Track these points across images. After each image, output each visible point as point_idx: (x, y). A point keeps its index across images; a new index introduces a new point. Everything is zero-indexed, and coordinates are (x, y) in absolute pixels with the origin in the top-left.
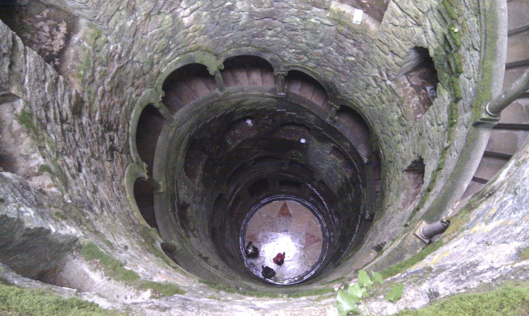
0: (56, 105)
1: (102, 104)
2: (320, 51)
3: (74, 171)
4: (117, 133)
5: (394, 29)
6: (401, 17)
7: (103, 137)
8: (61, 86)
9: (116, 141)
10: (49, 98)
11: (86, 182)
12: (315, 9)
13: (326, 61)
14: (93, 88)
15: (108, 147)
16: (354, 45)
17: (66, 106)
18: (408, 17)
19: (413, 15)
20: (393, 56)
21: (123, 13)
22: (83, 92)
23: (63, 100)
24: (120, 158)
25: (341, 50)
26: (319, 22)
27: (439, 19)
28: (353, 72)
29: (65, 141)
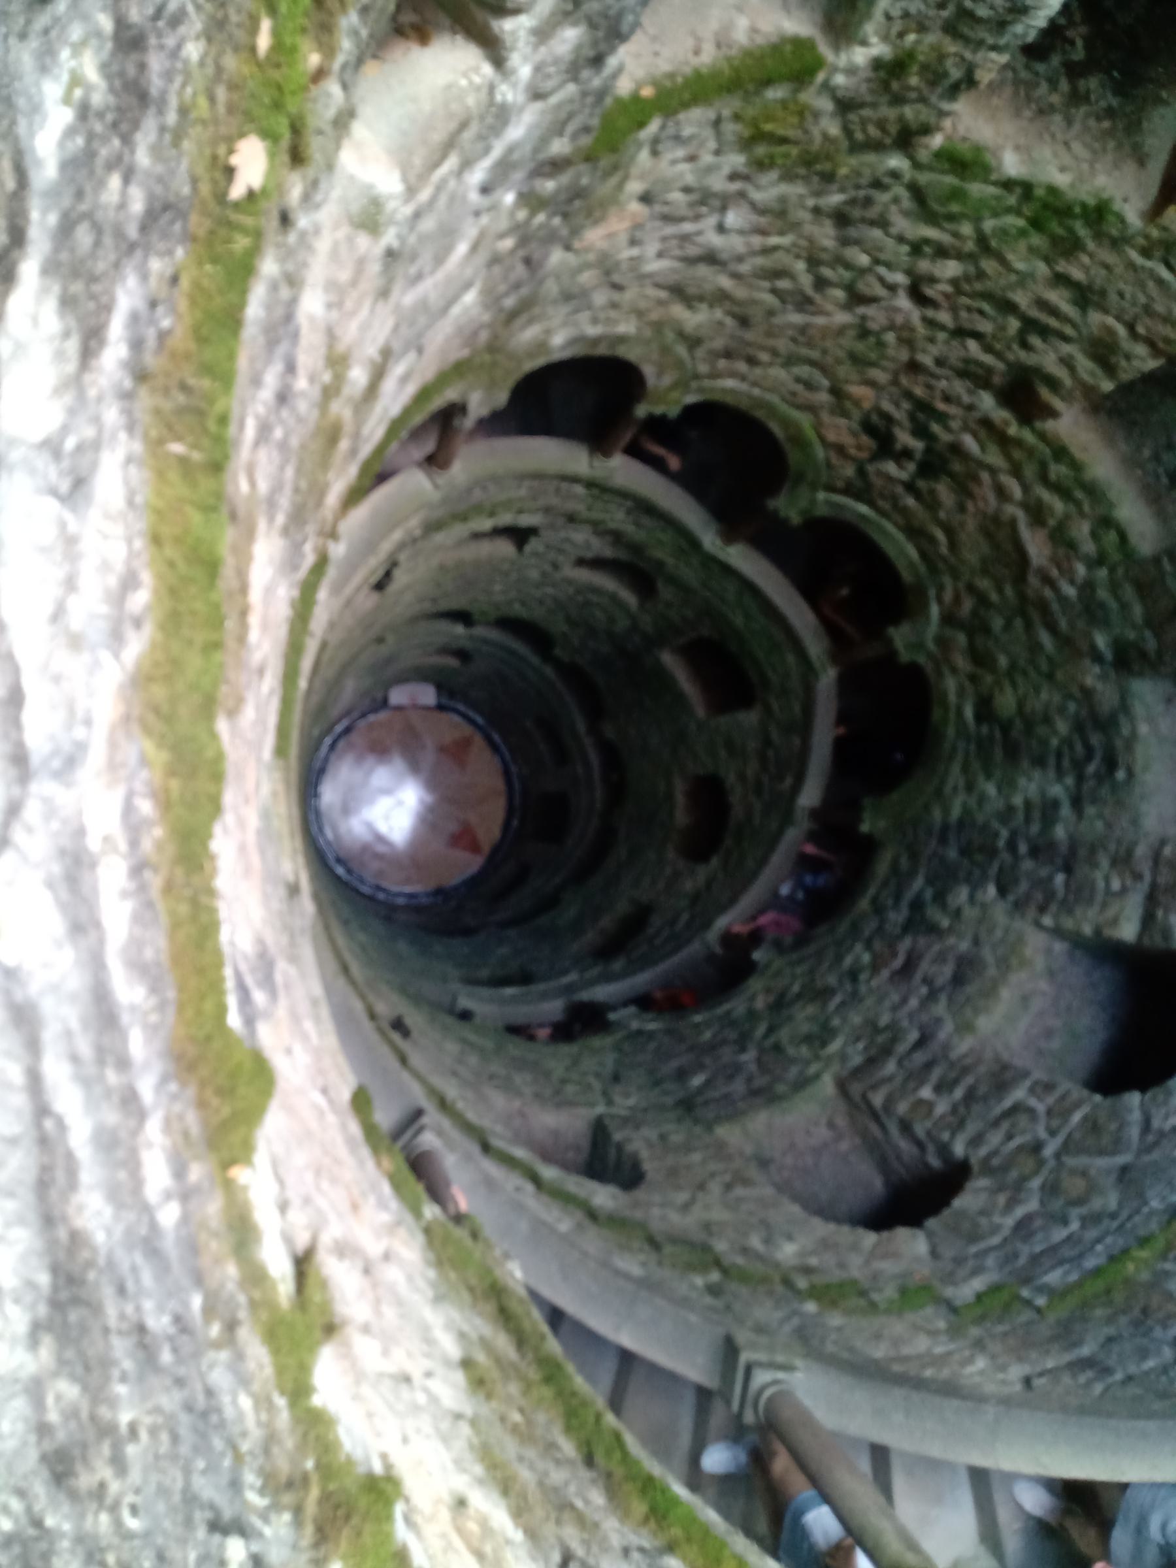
0: (1069, 331)
3: (924, 266)
7: (920, 431)
8: (1093, 374)
9: (891, 467)
10: (1096, 318)
11: (881, 280)
14: (1030, 471)
21: (1131, 635)
22: (1042, 436)
23: (1068, 363)
29: (987, 296)
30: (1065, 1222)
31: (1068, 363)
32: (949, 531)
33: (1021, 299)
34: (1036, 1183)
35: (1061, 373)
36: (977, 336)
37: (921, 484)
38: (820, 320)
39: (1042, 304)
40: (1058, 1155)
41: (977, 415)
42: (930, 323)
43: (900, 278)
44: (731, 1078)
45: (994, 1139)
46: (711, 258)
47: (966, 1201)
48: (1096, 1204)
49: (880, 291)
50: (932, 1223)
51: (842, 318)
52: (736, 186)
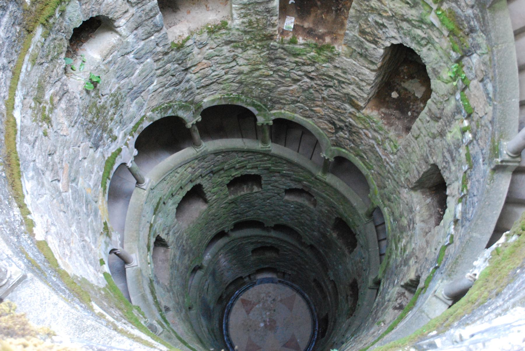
0: (348, 81)
1: (361, 131)
4: (347, 139)
7: (341, 120)
15: (334, 121)
17: (349, 90)
22: (363, 114)
23: (353, 90)
24: (330, 130)
31: (353, 90)
32: (366, 154)
33: (331, 74)
35: (353, 93)
36: (331, 87)
37: (351, 138)
38: (291, 88)
39: (336, 74)
41: (348, 111)
42: (316, 84)
43: (300, 73)
46: (240, 73)
49: (299, 78)
51: (295, 87)
52: (233, 53)
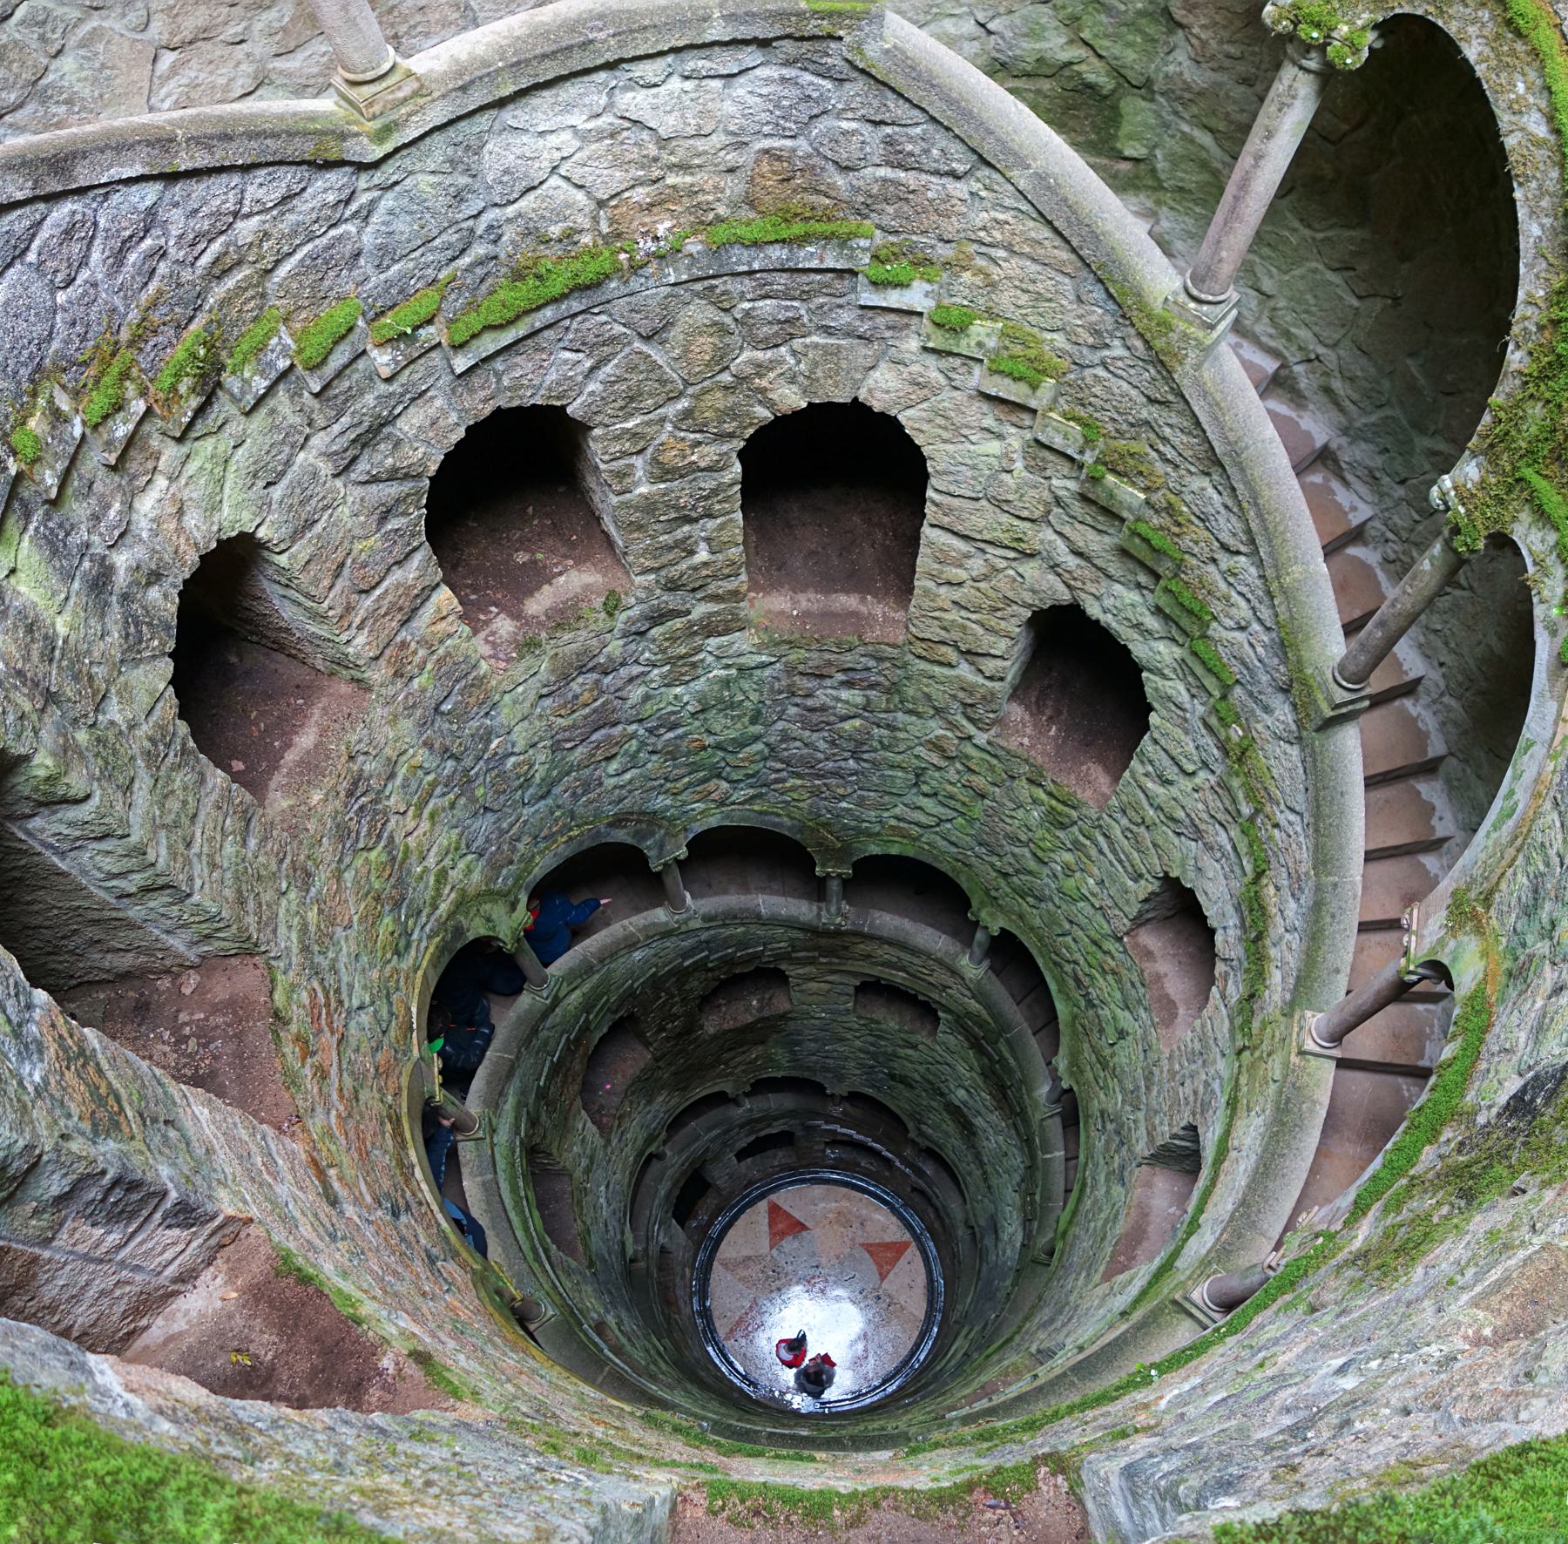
2: (759, 746)
5: (957, 594)
6: (968, 556)
12: (713, 642)
13: (779, 766)
16: (849, 684)
18: (989, 549)
19: (1005, 538)
20: (972, 664)
25: (815, 718)
26: (733, 671)
27: (1089, 520)
28: (865, 756)
30: (747, 313)
34: (726, 378)
40: (681, 394)
44: (823, 709)
45: (708, 454)
47: (792, 399)
48: (712, 314)
50: (842, 397)
